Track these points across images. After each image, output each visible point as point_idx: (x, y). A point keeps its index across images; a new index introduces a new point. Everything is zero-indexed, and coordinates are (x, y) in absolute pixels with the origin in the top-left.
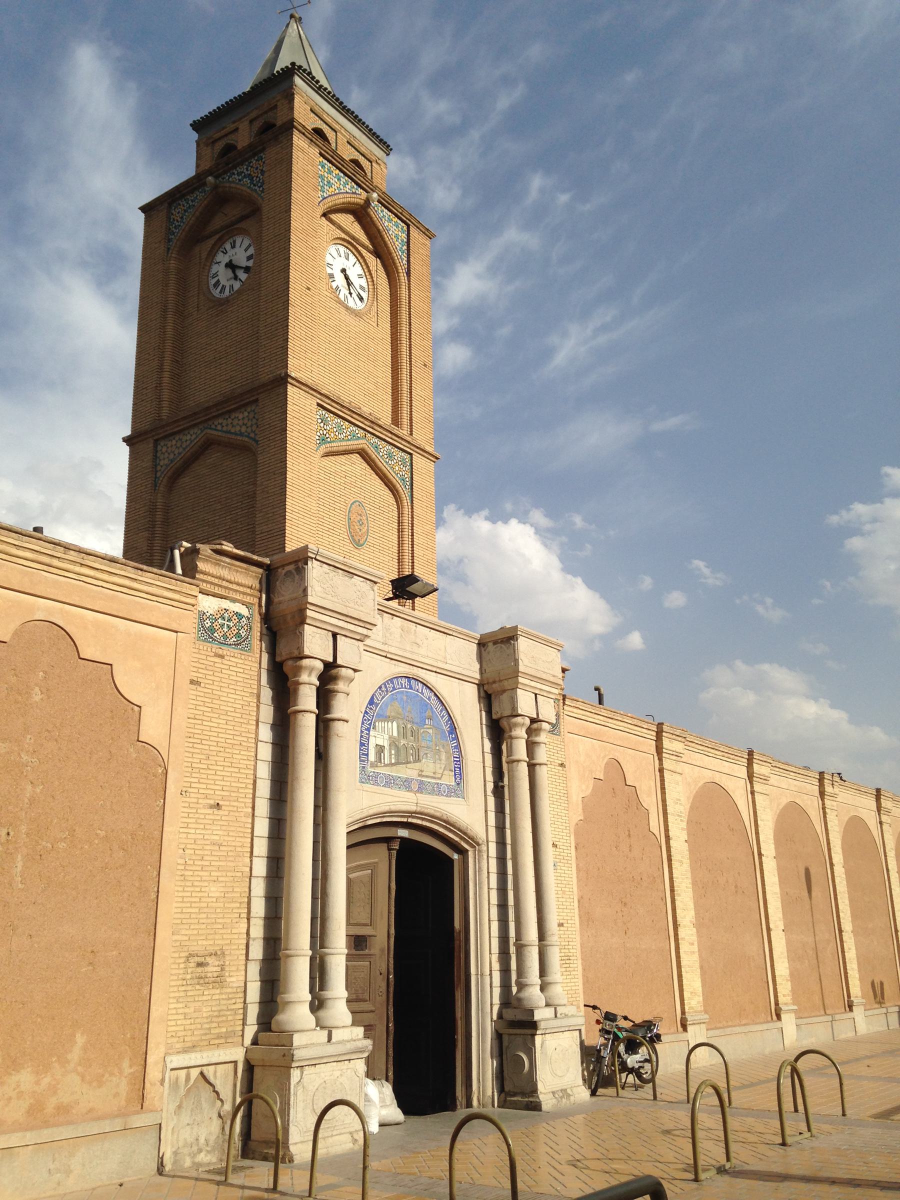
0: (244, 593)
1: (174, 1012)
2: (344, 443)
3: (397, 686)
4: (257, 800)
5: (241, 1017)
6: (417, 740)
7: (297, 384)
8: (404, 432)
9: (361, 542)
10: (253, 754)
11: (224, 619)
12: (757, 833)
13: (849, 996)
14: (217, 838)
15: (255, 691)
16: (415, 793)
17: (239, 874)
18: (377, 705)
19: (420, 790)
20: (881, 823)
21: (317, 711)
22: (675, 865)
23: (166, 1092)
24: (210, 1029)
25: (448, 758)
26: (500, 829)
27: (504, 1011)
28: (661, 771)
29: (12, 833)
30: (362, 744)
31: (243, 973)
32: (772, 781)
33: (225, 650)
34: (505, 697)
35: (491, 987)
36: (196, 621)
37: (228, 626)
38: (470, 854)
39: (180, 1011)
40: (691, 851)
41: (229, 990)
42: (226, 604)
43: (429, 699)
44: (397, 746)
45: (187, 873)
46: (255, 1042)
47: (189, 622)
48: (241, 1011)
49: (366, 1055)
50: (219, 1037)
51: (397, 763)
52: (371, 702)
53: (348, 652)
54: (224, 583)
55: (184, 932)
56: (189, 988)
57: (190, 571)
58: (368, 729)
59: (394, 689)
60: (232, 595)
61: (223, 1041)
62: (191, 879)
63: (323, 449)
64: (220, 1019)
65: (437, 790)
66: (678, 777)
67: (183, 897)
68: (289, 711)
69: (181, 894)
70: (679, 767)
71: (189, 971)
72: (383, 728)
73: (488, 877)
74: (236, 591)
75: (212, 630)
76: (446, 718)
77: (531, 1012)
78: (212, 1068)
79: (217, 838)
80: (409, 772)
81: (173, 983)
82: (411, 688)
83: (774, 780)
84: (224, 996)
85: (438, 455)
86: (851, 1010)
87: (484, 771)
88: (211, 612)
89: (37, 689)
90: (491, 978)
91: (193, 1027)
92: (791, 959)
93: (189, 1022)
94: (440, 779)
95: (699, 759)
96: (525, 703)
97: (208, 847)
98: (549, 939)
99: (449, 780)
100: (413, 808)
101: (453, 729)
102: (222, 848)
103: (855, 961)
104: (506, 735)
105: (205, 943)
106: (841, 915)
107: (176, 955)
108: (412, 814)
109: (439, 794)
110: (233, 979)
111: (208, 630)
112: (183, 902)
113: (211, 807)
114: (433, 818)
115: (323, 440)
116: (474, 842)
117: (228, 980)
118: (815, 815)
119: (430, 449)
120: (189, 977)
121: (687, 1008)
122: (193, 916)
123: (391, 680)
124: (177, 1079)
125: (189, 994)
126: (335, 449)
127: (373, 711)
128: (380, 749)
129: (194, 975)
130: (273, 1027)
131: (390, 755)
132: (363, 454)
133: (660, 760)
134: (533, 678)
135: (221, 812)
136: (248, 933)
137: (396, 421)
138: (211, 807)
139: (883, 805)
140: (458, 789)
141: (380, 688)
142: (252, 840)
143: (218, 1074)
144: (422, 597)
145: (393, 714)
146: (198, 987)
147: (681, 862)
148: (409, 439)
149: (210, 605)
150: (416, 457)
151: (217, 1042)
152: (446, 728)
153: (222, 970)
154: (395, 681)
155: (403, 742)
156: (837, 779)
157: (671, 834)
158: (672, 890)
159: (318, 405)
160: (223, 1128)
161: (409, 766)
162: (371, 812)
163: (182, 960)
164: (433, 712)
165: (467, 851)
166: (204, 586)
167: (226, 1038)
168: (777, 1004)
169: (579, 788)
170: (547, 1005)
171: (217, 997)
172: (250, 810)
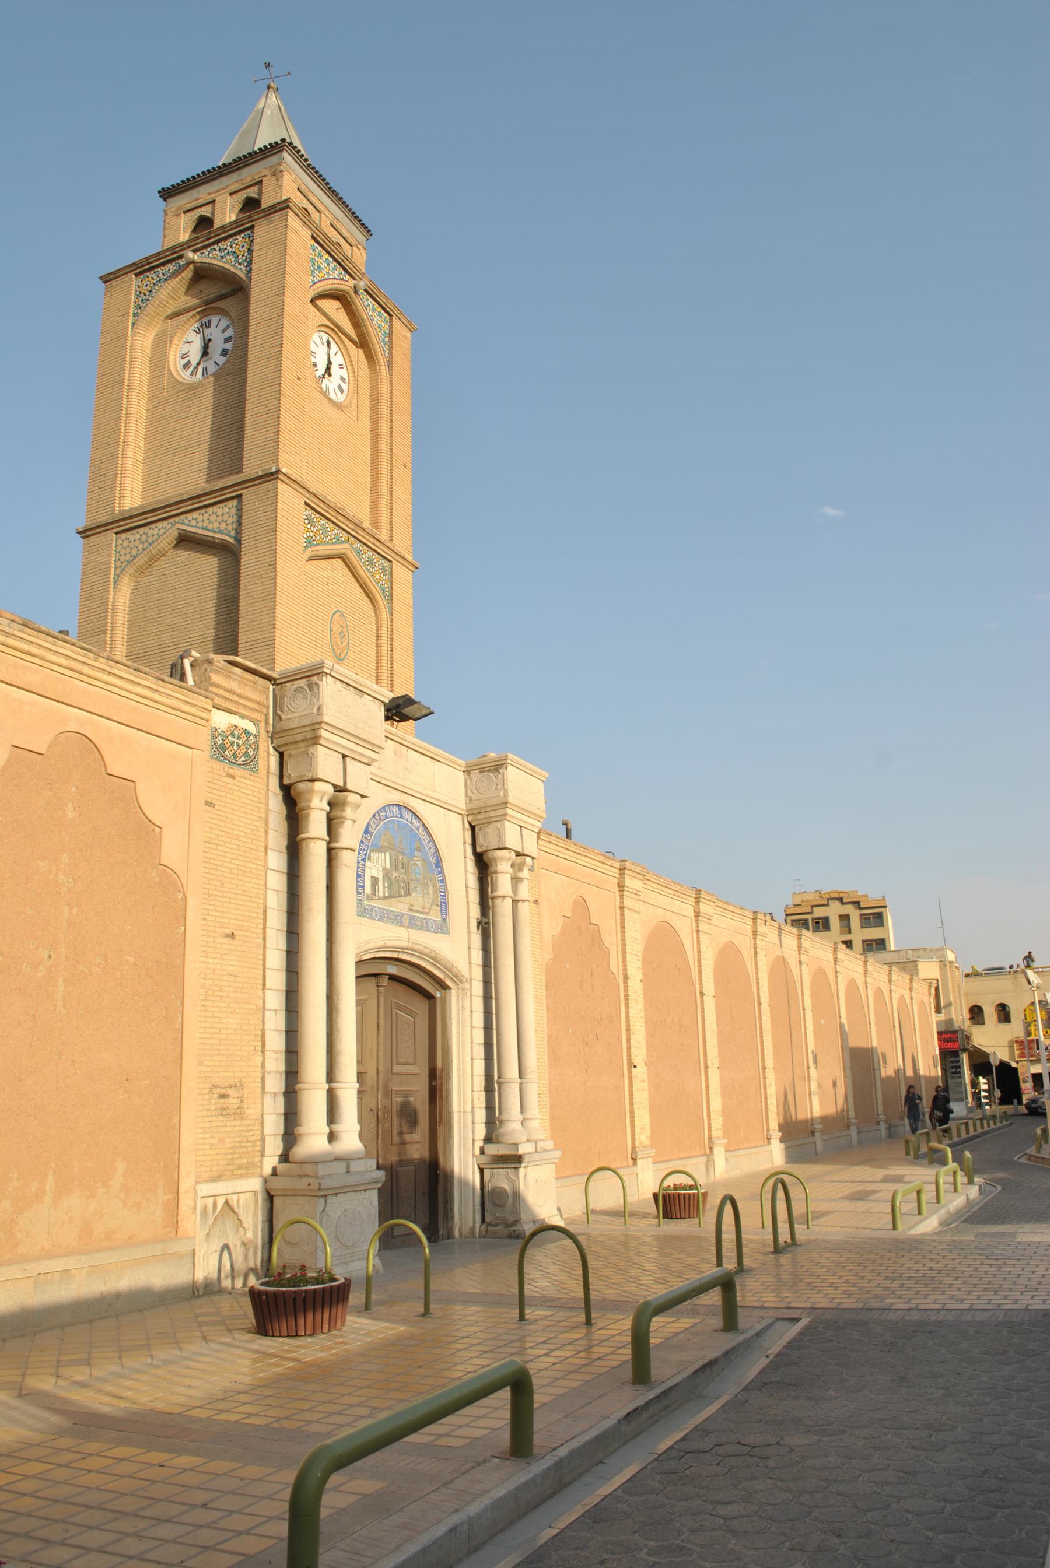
0: (252, 709)
1: (201, 1141)
2: (329, 547)
3: (389, 815)
4: (268, 930)
5: (259, 1148)
6: (407, 873)
7: (287, 481)
8: (384, 536)
9: (342, 656)
10: (263, 882)
11: (234, 736)
12: (700, 972)
13: (768, 1130)
14: (232, 968)
15: (263, 816)
16: (406, 927)
17: (253, 1007)
18: (371, 834)
19: (411, 926)
20: (800, 962)
21: (327, 838)
22: (632, 1004)
23: (198, 1218)
24: (232, 1160)
25: (435, 893)
26: (486, 965)
27: (486, 1146)
28: (622, 908)
29: (53, 956)
30: (358, 876)
31: (260, 1105)
32: (715, 921)
33: (236, 771)
34: (491, 830)
35: (473, 1123)
36: (210, 738)
37: (238, 744)
38: (453, 992)
39: (207, 1141)
40: (645, 990)
41: (248, 1122)
42: (235, 720)
43: (418, 829)
44: (390, 879)
45: (208, 1004)
46: (274, 1173)
47: (204, 740)
48: (259, 1143)
49: (379, 1185)
50: (241, 1167)
51: (390, 897)
52: (367, 831)
53: (358, 777)
54: (235, 698)
55: (207, 1063)
56: (214, 1119)
57: (204, 685)
58: (364, 860)
59: (387, 817)
60: (242, 711)
61: (244, 1171)
62: (211, 1009)
63: (309, 553)
64: (241, 1150)
65: (425, 926)
66: (636, 916)
67: (205, 1028)
68: (298, 838)
69: (203, 1025)
70: (637, 906)
71: (213, 1102)
72: (377, 859)
73: (471, 1016)
74: (245, 706)
75: (223, 748)
76: (433, 850)
77: (516, 1145)
78: (235, 1197)
79: (232, 968)
80: (399, 906)
81: (200, 1114)
82: (401, 817)
83: (715, 920)
84: (243, 1128)
85: (417, 564)
86: (769, 1143)
87: (468, 908)
88: (223, 728)
89: (70, 805)
90: (473, 1115)
91: (217, 1157)
92: (724, 1096)
93: (214, 1152)
94: (428, 914)
95: (661, 900)
96: (512, 836)
97: (225, 978)
98: (529, 1076)
99: (435, 916)
100: (405, 944)
101: (439, 863)
102: (238, 979)
103: (774, 1097)
104: (492, 869)
105: (225, 1074)
106: (765, 1052)
107: (201, 1086)
108: (404, 950)
109: (428, 930)
110: (251, 1111)
111: (221, 748)
112: (205, 1033)
113: (227, 936)
114: (421, 954)
115: (309, 543)
116: (458, 978)
117: (247, 1112)
118: (747, 954)
119: (410, 558)
120: (213, 1107)
121: (637, 1142)
122: (215, 1047)
123: (384, 808)
124: (206, 1207)
125: (214, 1124)
126: (320, 553)
127: (369, 843)
128: (375, 881)
129: (218, 1106)
130: (291, 1159)
131: (384, 887)
132: (343, 557)
133: (621, 896)
134: (521, 810)
135: (235, 942)
136: (263, 1066)
137: (375, 523)
138: (227, 936)
139: (803, 945)
140: (442, 927)
141: (374, 816)
142: (264, 972)
143: (241, 1203)
144: (415, 720)
145: (386, 844)
146: (221, 1118)
147: (636, 1001)
148: (389, 545)
149: (221, 720)
150: (395, 564)
151: (240, 1172)
152: (433, 861)
153: (242, 1101)
154: (387, 809)
155: (395, 874)
156: (768, 918)
157: (629, 973)
158: (628, 1030)
159: (306, 504)
160: (246, 1255)
161: (401, 899)
162: (369, 947)
163: (207, 1091)
164: (421, 843)
165: (450, 988)
166: (218, 701)
167: (247, 1168)
168: (710, 1138)
169: (552, 928)
170: (528, 1141)
171: (237, 1128)
172: (261, 941)
